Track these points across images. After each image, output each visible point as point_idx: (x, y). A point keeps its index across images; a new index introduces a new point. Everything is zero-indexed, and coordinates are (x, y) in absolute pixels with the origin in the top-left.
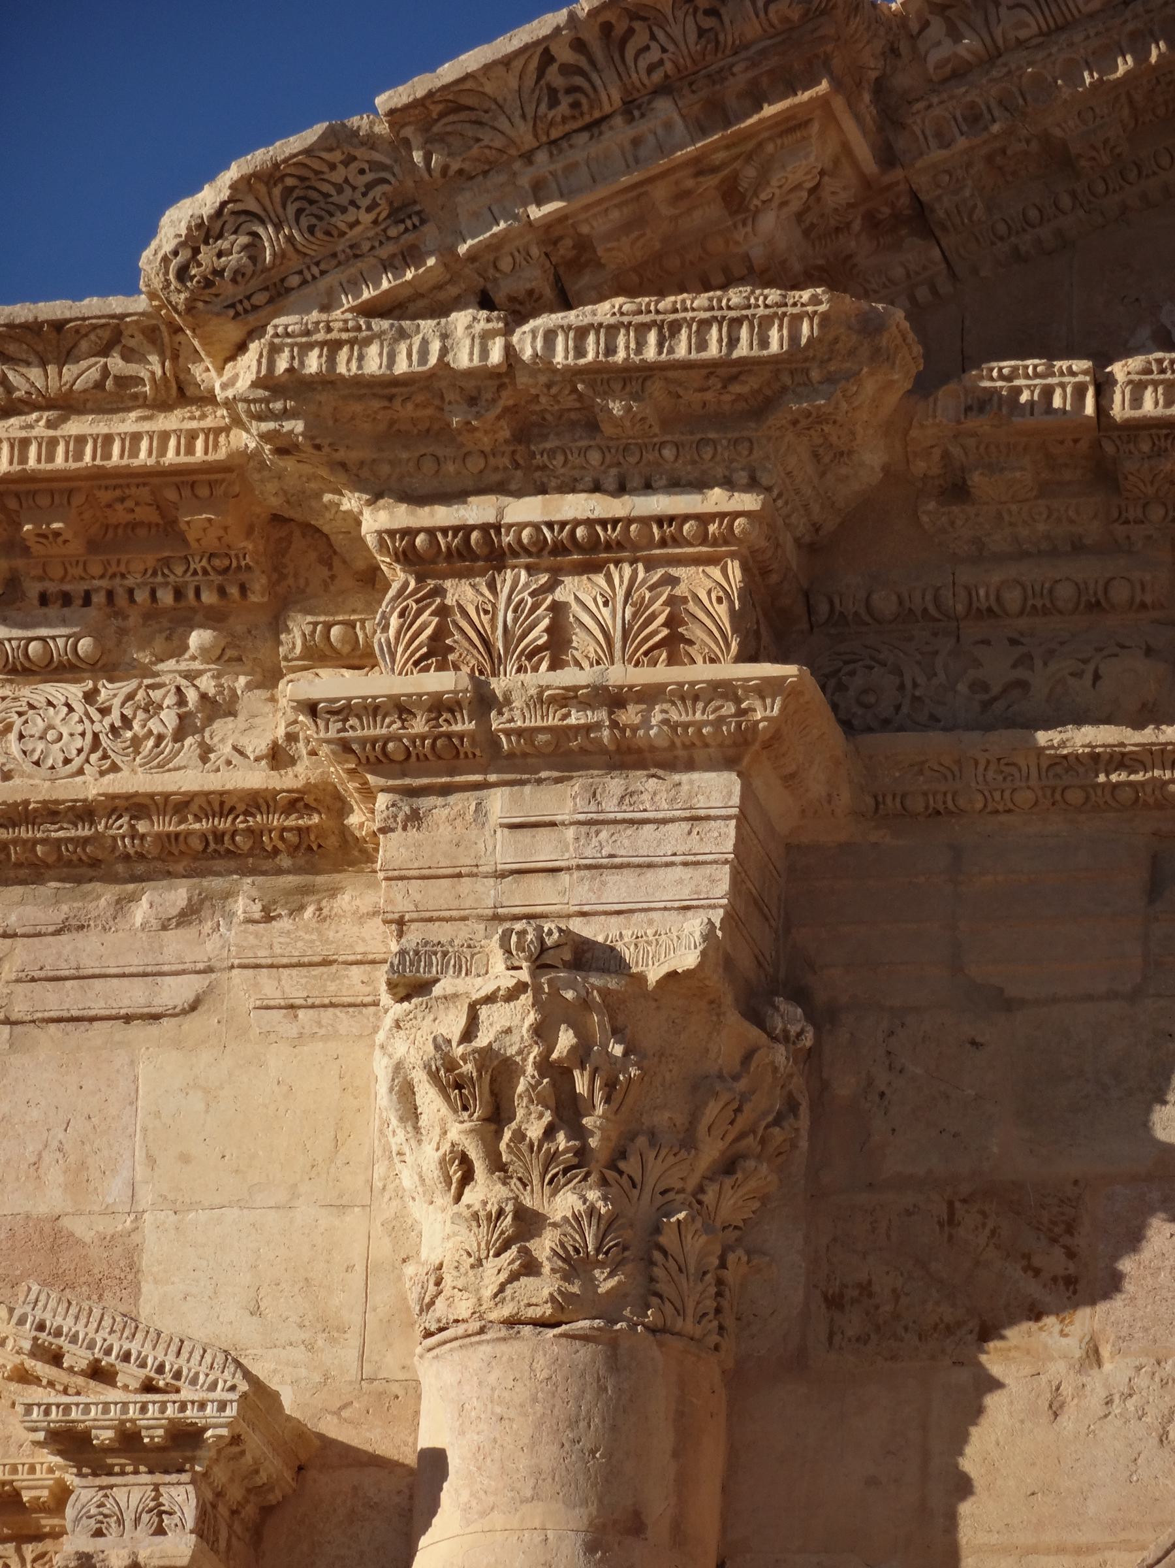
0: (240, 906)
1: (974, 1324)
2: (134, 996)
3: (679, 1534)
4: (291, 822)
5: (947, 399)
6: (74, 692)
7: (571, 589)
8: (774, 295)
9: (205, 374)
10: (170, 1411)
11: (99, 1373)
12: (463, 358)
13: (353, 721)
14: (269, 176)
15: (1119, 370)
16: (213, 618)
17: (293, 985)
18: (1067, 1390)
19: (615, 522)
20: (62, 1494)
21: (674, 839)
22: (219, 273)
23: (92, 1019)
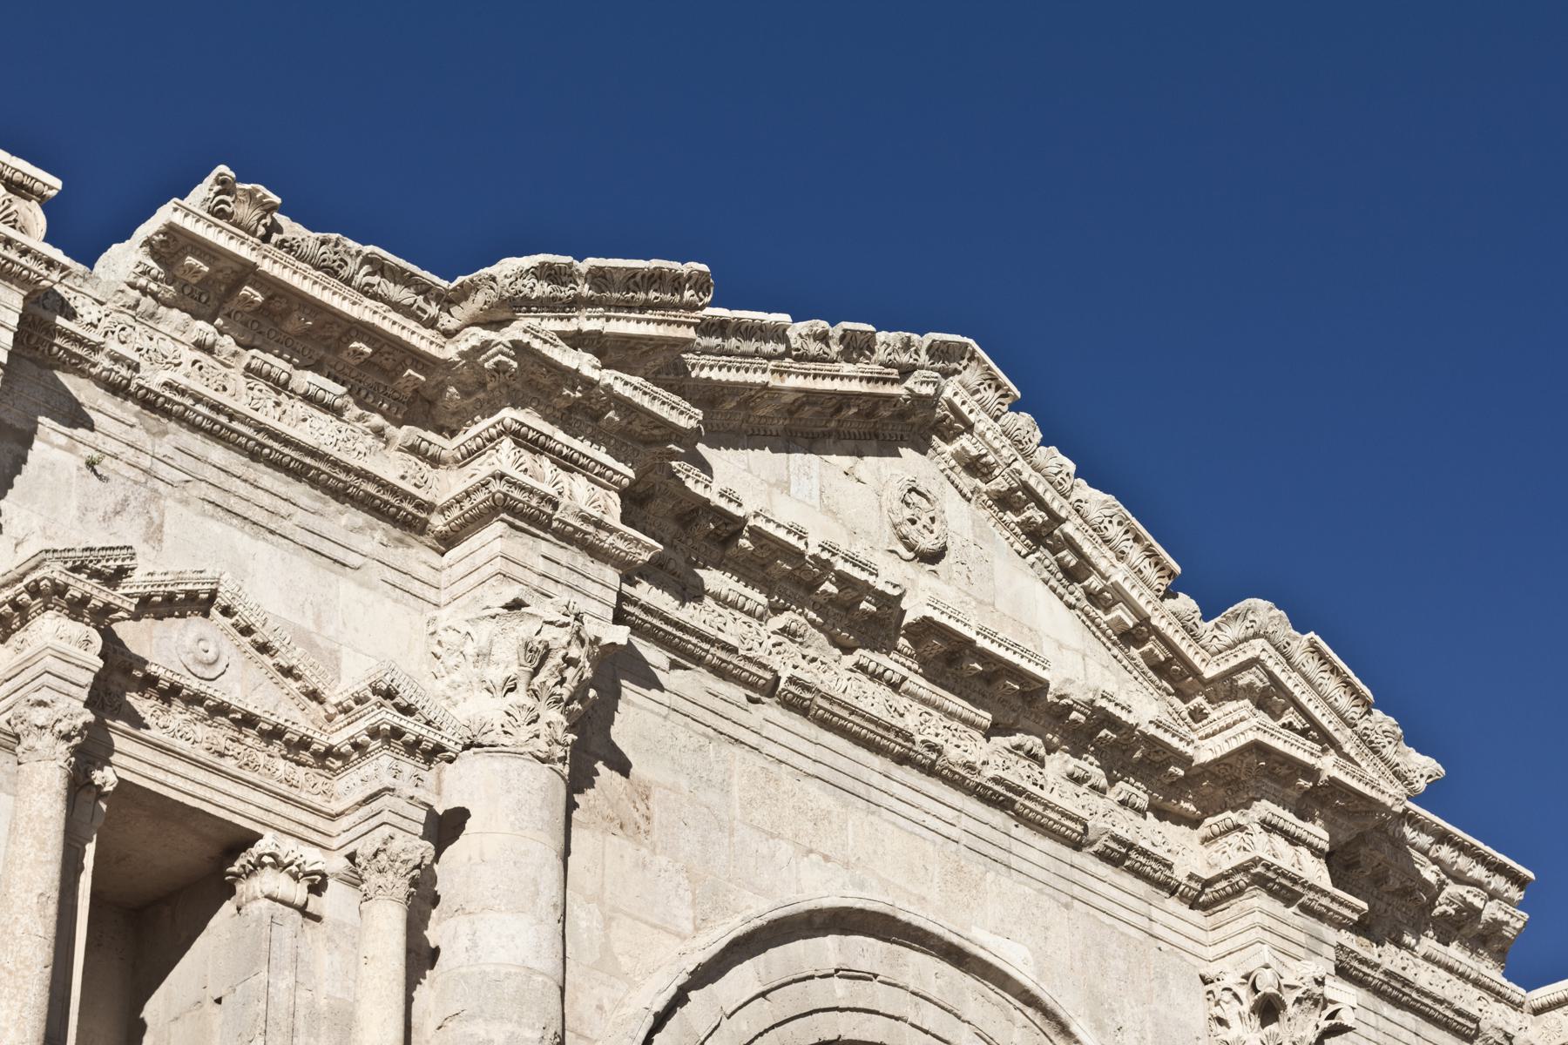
0: (379, 535)
1: (618, 821)
2: (339, 553)
4: (415, 511)
8: (688, 405)
10: (438, 738)
11: (408, 710)
12: (587, 371)
13: (513, 489)
14: (551, 266)
16: (385, 415)
18: (647, 860)
19: (588, 458)
21: (595, 589)
22: (521, 292)
23: (323, 555)
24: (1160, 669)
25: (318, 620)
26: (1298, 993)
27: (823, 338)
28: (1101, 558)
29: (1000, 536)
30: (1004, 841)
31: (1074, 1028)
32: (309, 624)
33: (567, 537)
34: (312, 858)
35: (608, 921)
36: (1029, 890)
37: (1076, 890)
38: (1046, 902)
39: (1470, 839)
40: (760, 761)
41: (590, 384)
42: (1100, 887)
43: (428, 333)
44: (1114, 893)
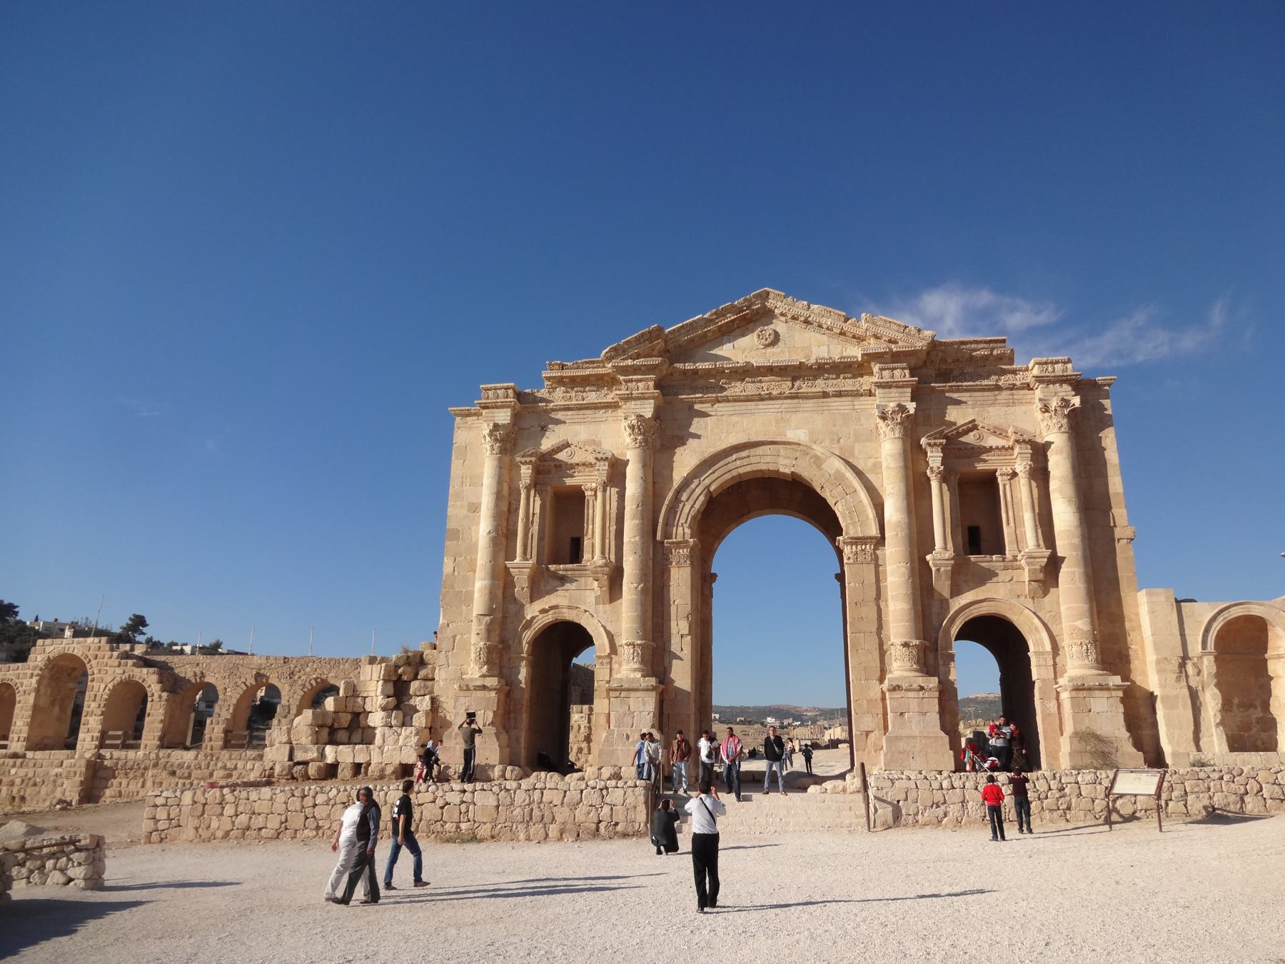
2: (600, 420)
3: (650, 466)
5: (671, 368)
6: (594, 393)
7: (639, 384)
9: (606, 365)
11: (599, 453)
12: (629, 364)
14: (612, 348)
15: (686, 364)
17: (615, 419)
20: (596, 463)
24: (854, 337)
25: (596, 436)
26: (890, 413)
27: (715, 313)
28: (823, 321)
29: (798, 327)
30: (798, 405)
31: (813, 447)
32: (594, 437)
33: (638, 398)
34: (594, 485)
37: (825, 408)
39: (971, 339)
40: (716, 417)
41: (631, 366)
42: (834, 404)
43: (604, 369)
44: (839, 404)
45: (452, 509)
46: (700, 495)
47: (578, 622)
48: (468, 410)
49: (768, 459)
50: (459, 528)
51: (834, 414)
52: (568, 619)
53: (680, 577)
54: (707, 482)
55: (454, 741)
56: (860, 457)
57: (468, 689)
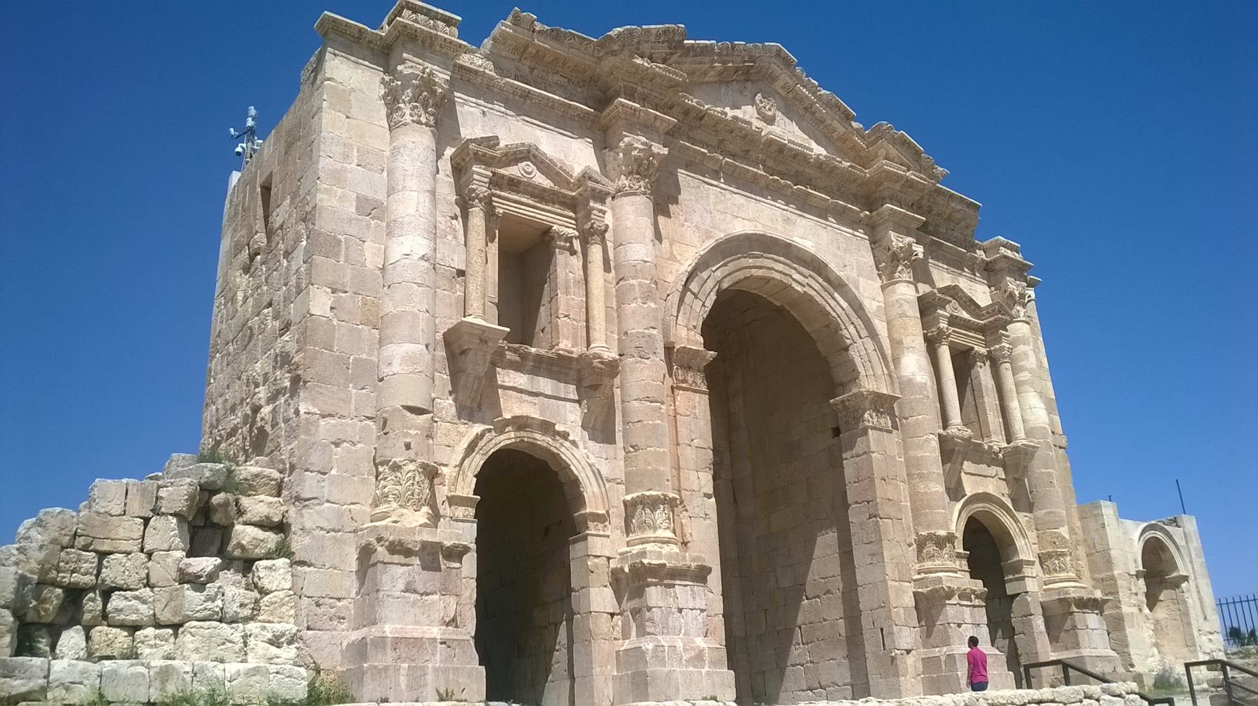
12: (646, 64)
25: (565, 156)
35: (671, 245)
36: (812, 223)
38: (818, 227)
45: (325, 196)
46: (711, 291)
47: (556, 451)
48: (360, 30)
49: (780, 267)
50: (339, 237)
51: (837, 233)
52: (539, 442)
53: (697, 405)
54: (719, 274)
55: (390, 654)
56: (866, 295)
57: (408, 553)
